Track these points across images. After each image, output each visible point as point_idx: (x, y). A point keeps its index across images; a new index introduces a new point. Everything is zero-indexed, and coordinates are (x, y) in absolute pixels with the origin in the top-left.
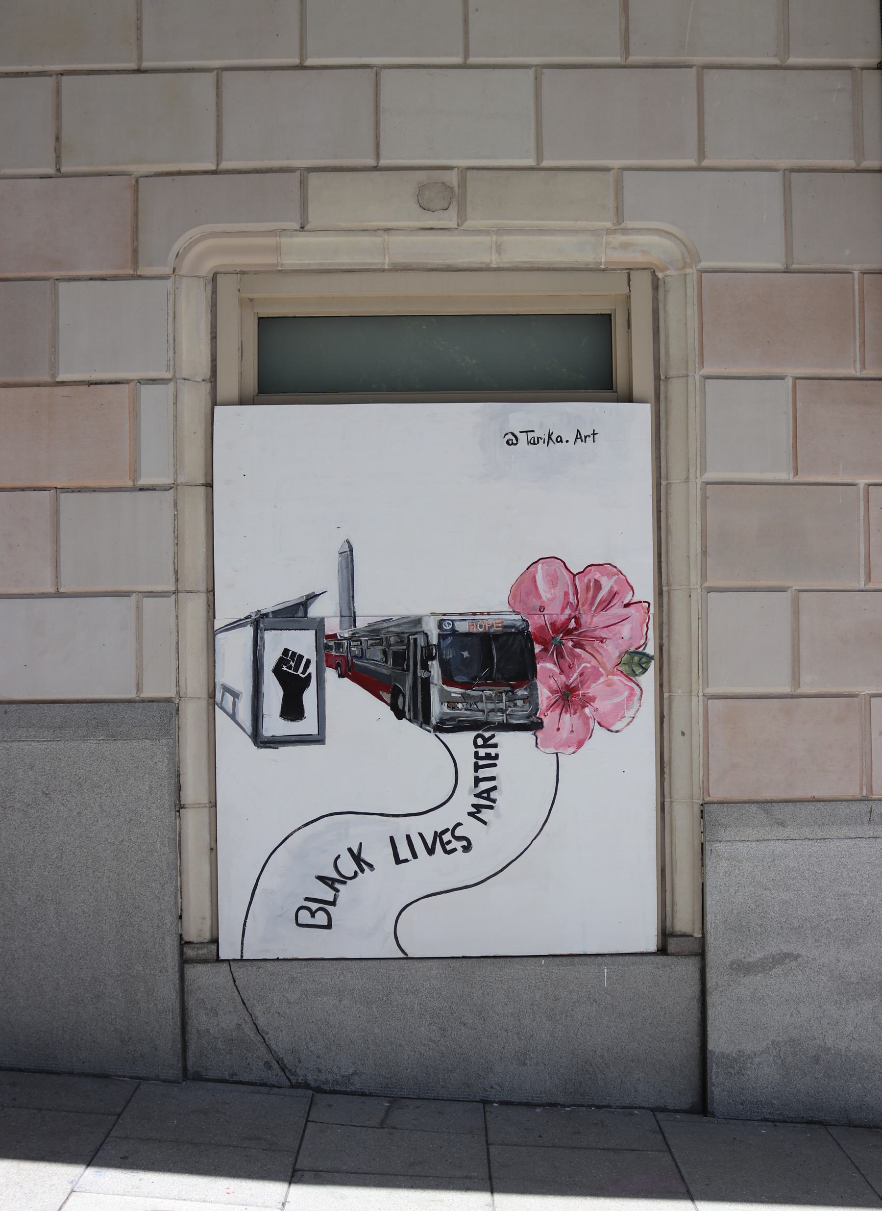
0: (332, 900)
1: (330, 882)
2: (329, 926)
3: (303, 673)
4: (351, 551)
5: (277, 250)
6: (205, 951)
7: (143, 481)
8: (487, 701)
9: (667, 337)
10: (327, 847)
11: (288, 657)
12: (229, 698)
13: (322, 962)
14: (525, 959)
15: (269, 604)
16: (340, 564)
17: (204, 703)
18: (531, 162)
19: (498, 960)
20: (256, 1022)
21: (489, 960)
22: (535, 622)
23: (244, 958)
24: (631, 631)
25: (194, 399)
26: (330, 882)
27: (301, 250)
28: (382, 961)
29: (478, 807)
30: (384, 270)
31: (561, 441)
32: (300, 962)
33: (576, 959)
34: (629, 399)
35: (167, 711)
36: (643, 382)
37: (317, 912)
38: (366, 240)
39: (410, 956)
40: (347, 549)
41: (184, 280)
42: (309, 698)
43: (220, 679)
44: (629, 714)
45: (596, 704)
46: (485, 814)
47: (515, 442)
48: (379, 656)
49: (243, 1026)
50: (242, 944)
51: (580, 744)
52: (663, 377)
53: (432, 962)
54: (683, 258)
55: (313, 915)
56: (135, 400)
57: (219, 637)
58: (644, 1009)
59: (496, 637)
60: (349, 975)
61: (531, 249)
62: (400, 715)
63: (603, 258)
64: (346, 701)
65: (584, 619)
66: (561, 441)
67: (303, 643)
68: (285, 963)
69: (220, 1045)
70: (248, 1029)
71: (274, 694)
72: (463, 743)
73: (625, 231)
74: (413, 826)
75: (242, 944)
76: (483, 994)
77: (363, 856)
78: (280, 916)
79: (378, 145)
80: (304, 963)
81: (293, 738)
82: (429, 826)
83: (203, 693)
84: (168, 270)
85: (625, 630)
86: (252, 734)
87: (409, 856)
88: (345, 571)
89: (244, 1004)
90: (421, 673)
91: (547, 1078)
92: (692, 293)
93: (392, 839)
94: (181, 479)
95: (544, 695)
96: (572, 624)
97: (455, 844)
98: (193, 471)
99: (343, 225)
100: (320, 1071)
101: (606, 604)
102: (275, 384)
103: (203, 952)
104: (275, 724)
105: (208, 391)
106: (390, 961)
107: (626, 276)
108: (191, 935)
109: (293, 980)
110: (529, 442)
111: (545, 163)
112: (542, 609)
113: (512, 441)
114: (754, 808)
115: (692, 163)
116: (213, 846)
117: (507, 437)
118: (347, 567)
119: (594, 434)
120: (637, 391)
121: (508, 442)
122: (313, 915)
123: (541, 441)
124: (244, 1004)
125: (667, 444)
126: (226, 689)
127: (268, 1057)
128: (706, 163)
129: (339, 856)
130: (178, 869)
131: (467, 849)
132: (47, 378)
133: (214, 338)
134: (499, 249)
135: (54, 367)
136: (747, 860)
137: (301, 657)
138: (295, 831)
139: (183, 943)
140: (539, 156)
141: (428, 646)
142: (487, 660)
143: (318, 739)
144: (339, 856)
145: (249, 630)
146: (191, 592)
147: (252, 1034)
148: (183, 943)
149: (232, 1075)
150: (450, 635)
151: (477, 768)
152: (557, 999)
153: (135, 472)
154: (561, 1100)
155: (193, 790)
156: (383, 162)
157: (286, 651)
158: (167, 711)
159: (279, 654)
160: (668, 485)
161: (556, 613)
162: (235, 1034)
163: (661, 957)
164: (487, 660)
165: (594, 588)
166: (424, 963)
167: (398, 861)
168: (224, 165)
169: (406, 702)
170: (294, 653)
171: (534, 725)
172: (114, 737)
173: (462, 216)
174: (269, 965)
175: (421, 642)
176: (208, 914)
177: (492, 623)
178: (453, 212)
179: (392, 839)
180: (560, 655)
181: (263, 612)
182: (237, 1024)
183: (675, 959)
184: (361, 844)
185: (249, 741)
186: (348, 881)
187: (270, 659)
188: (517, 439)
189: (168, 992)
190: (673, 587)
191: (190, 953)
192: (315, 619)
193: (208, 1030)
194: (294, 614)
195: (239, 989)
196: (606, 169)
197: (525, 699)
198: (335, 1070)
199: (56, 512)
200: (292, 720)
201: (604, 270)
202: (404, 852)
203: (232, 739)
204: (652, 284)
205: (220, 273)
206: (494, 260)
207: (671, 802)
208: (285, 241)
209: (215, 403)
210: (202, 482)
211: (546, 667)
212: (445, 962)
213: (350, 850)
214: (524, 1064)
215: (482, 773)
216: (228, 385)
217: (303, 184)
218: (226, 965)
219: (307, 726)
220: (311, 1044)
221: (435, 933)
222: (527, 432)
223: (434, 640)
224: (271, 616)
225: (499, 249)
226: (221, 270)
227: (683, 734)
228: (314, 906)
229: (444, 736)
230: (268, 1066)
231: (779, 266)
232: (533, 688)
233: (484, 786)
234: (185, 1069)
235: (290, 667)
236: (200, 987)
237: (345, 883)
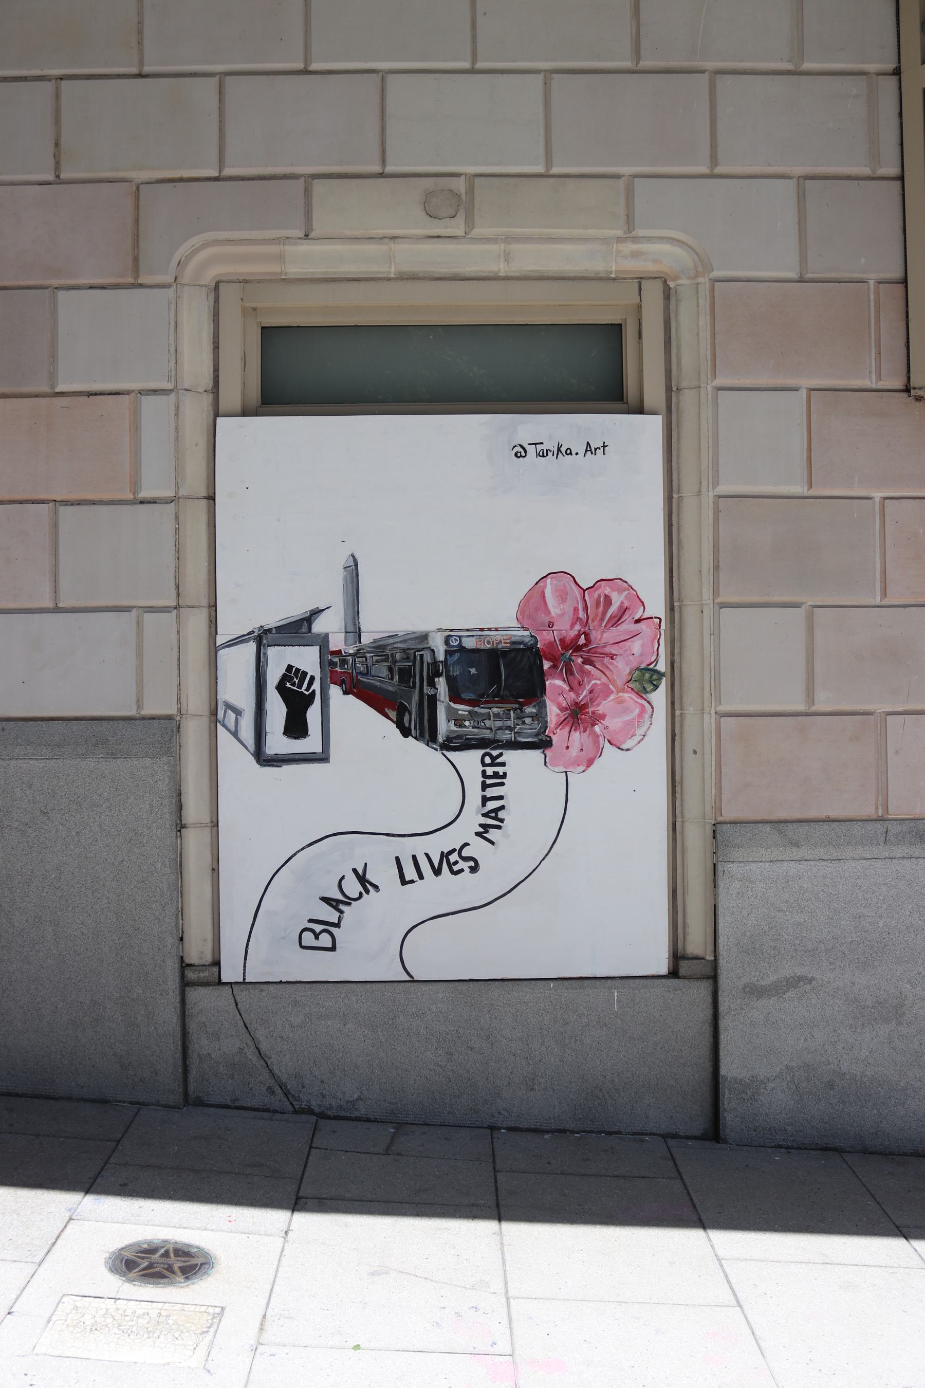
0: (336, 921)
1: (334, 904)
2: (333, 948)
3: (307, 690)
4: (356, 565)
5: (281, 258)
6: (207, 974)
7: (144, 494)
8: (495, 719)
9: (679, 348)
10: (331, 868)
11: (292, 674)
12: (232, 716)
13: (326, 985)
14: (533, 982)
15: (272, 620)
16: (345, 579)
17: (205, 721)
18: (540, 169)
19: (506, 983)
22: (544, 638)
24: (641, 648)
25: (195, 410)
26: (334, 904)
27: (306, 258)
29: (486, 827)
30: (390, 279)
31: (571, 454)
32: (304, 985)
33: (586, 982)
34: (640, 410)
35: (167, 729)
36: (654, 393)
37: (321, 934)
38: (371, 248)
39: (416, 979)
40: (351, 563)
41: (186, 288)
42: (313, 715)
43: (223, 696)
44: (641, 731)
45: (606, 722)
46: (493, 834)
47: (523, 454)
48: (385, 673)
50: (245, 966)
51: (590, 763)
52: (674, 389)
53: (438, 985)
55: (317, 936)
56: (136, 412)
57: (221, 653)
59: (504, 653)
61: (540, 258)
62: (406, 733)
63: (614, 267)
65: (594, 635)
66: (571, 454)
67: (307, 659)
70: (251, 1053)
72: (470, 762)
73: (635, 240)
74: (420, 846)
75: (245, 966)
76: (491, 1018)
78: (283, 938)
79: (383, 152)
80: (308, 985)
81: (297, 757)
82: (436, 846)
83: (205, 710)
84: (169, 279)
85: (636, 646)
87: (416, 877)
88: (350, 586)
90: (427, 690)
91: (556, 1103)
92: (704, 303)
93: (397, 859)
94: (183, 492)
95: (553, 712)
96: (582, 640)
97: (462, 865)
98: (195, 483)
99: (348, 233)
100: (324, 1096)
101: (617, 620)
102: (279, 394)
103: (205, 975)
106: (396, 984)
107: (637, 285)
108: (193, 958)
109: (296, 1003)
110: (538, 455)
111: (555, 170)
112: (551, 625)
114: (767, 828)
115: (704, 169)
117: (516, 449)
118: (352, 582)
119: (604, 446)
120: (648, 403)
121: (516, 455)
122: (317, 936)
123: (550, 454)
125: (678, 457)
126: (228, 706)
127: (271, 1082)
128: (718, 170)
130: (179, 890)
131: (474, 869)
132: (46, 389)
133: (216, 347)
134: (507, 257)
135: (53, 377)
136: (759, 882)
137: (305, 674)
138: (298, 852)
139: (184, 966)
140: (549, 162)
141: (435, 663)
142: (495, 677)
143: (322, 758)
145: (252, 646)
148: (184, 966)
149: (234, 1101)
150: (456, 651)
151: (484, 786)
153: (136, 485)
154: (571, 1126)
155: (195, 810)
156: (389, 169)
157: (290, 668)
158: (167, 729)
159: (283, 670)
160: (680, 499)
161: (565, 628)
162: (237, 1059)
164: (495, 677)
165: (605, 604)
167: (404, 882)
168: (227, 172)
169: (410, 719)
170: (298, 670)
171: (542, 744)
172: (114, 756)
173: (470, 224)
174: (272, 988)
175: (428, 658)
176: (209, 936)
177: (500, 639)
178: (460, 219)
179: (397, 859)
180: (569, 671)
181: (266, 628)
182: (239, 1048)
183: (686, 982)
185: (252, 759)
189: (168, 1014)
190: (685, 603)
191: (191, 975)
192: (319, 635)
193: (209, 1054)
194: (298, 630)
196: (617, 177)
197: (533, 717)
198: (340, 1095)
199: (55, 526)
200: (296, 738)
201: (614, 279)
202: (410, 873)
203: (235, 757)
205: (223, 282)
206: (502, 269)
207: (683, 822)
208: (289, 249)
209: (217, 414)
210: (204, 495)
211: (555, 683)
212: (452, 985)
213: (355, 871)
214: (533, 1089)
215: (490, 792)
216: (231, 396)
217: (308, 192)
218: (228, 988)
219: (311, 744)
221: (444, 955)
222: (536, 444)
223: (441, 657)
224: (274, 631)
225: (507, 257)
227: (695, 752)
228: (318, 928)
229: (451, 755)
230: (271, 1091)
231: (793, 275)
232: (542, 706)
233: (491, 805)
234: (186, 1094)
235: (293, 684)
236: (201, 1011)
237: (349, 904)
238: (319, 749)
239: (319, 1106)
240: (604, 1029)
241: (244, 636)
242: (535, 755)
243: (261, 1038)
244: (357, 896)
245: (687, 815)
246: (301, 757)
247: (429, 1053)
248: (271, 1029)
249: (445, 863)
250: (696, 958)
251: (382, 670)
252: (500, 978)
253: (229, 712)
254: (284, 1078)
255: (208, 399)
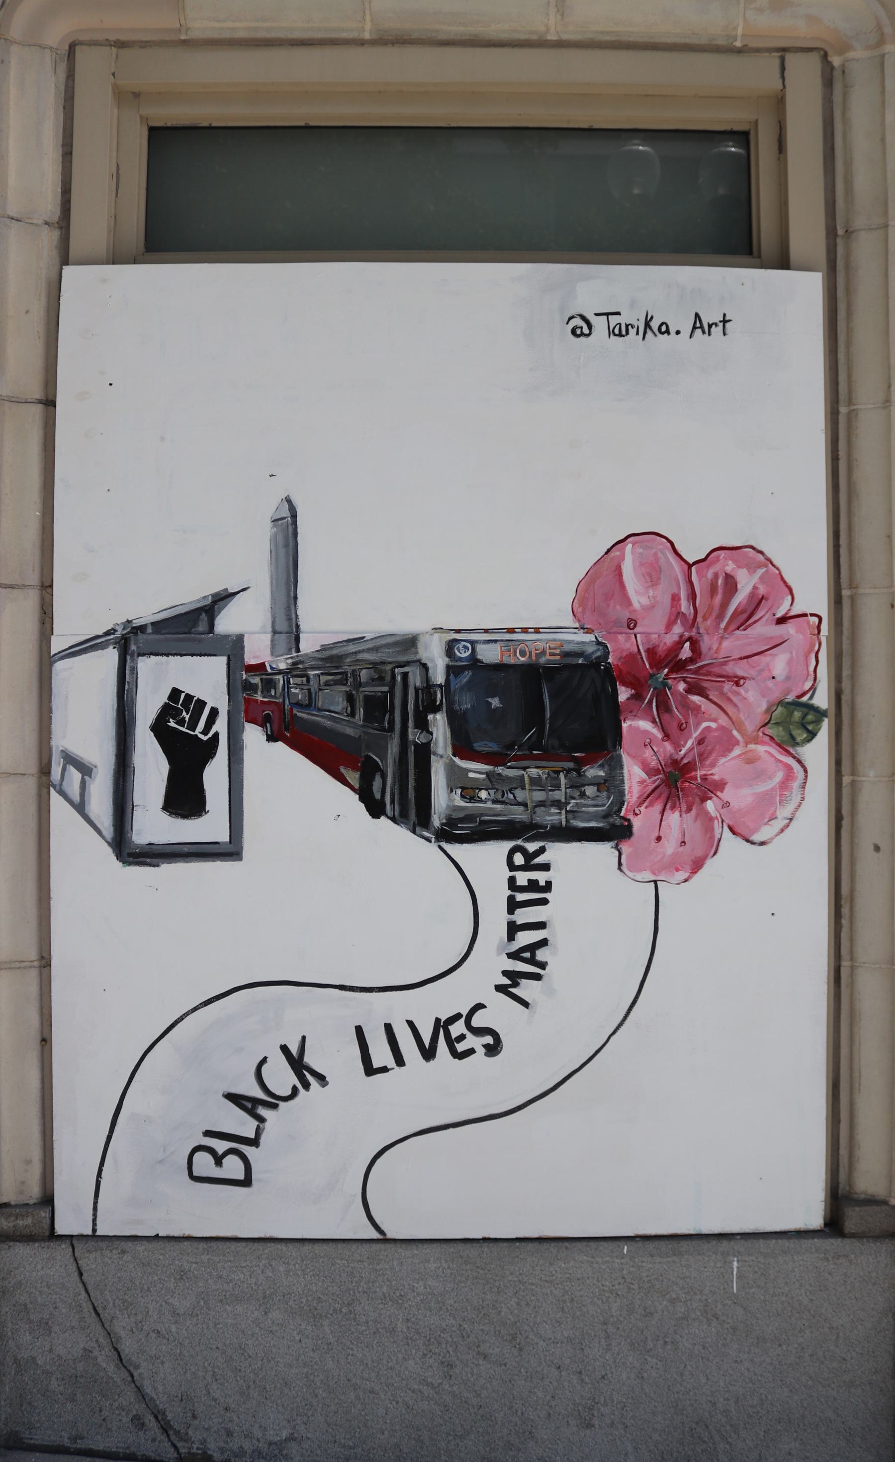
0: (253, 1136)
1: (249, 1105)
2: (247, 1182)
3: (205, 732)
4: (294, 516)
6: (29, 1221)
8: (532, 785)
9: (848, 163)
11: (179, 704)
13: (233, 1246)
14: (593, 1244)
16: (274, 540)
17: (31, 784)
19: (546, 1245)
20: (118, 1347)
21: (530, 1246)
22: (620, 647)
23: (98, 1233)
26: (249, 1105)
28: (340, 1246)
29: (514, 977)
30: (362, 43)
31: (668, 332)
32: (195, 1244)
33: (685, 1245)
39: (389, 1235)
40: (285, 512)
41: (15, 49)
44: (784, 812)
45: (727, 794)
46: (526, 989)
47: (586, 330)
48: (340, 704)
49: (96, 1353)
50: (95, 1209)
51: (697, 866)
52: (840, 232)
53: (427, 1249)
54: (879, 27)
55: (218, 1160)
57: (60, 667)
58: (801, 1331)
60: (282, 1269)
62: (375, 809)
64: (281, 784)
65: (707, 643)
66: (668, 332)
67: (205, 679)
68: (169, 1246)
69: (54, 1385)
71: (152, 767)
72: (488, 861)
74: (398, 1009)
75: (95, 1209)
76: (518, 1304)
77: (308, 1059)
78: (161, 1162)
80: (202, 1245)
81: (186, 849)
82: (427, 1008)
85: (779, 663)
86: (114, 839)
87: (390, 1062)
88: (282, 551)
89: (98, 1314)
90: (415, 736)
91: (630, 1449)
93: (359, 1030)
95: (634, 776)
96: (686, 652)
97: (472, 1041)
100: (229, 1433)
101: (746, 618)
104: (153, 824)
105: (55, 243)
106: (354, 1246)
107: (777, 62)
109: (182, 1275)
110: (611, 333)
112: (632, 624)
113: (581, 329)
116: (46, 1036)
117: (573, 323)
118: (286, 546)
119: (725, 321)
120: (796, 250)
121: (573, 332)
122: (218, 1160)
123: (632, 332)
124: (98, 1314)
125: (848, 344)
127: (139, 1408)
129: (264, 1060)
131: (493, 1050)
133: (67, 154)
137: (201, 704)
138: (187, 1014)
141: (428, 687)
142: (533, 713)
143: (230, 851)
144: (264, 1060)
145: (111, 655)
146: (11, 587)
147: (109, 1366)
149: (74, 1439)
150: (467, 667)
151: (513, 905)
152: (648, 1314)
157: (175, 693)
159: (164, 699)
160: (852, 416)
161: (656, 631)
162: (80, 1367)
163: (832, 1241)
164: (533, 713)
165: (725, 590)
166: (415, 1250)
167: (370, 1070)
169: (385, 787)
170: (189, 697)
171: (615, 831)
174: (141, 1247)
175: (416, 679)
176: (36, 1155)
179: (359, 1030)
180: (664, 706)
181: (136, 623)
182: (85, 1350)
183: (856, 1243)
184: (304, 1038)
185: (108, 852)
186: (282, 1104)
187: (147, 708)
188: (590, 326)
190: (861, 591)
192: (226, 637)
193: (34, 1359)
194: (190, 628)
195: (90, 1288)
197: (600, 785)
198: (258, 1433)
200: (185, 817)
201: (740, 51)
202: (381, 1055)
204: (823, 76)
205: (81, 43)
207: (852, 968)
210: (39, 397)
211: (638, 726)
212: (451, 1249)
213: (284, 1049)
214: (589, 1426)
215: (523, 916)
218: (65, 1247)
219: (211, 827)
220: (214, 1386)
222: (607, 314)
223: (439, 678)
224: (149, 630)
226: (82, 38)
227: (877, 848)
228: (221, 1146)
229: (454, 849)
230: (138, 1422)
232: (616, 765)
233: (525, 938)
235: (181, 722)
236: (20, 1283)
237: (274, 1106)
238: (222, 835)
239: (222, 1450)
240: (714, 1323)
241: (98, 637)
242: (604, 851)
243: (122, 1334)
244: (288, 1092)
245: (862, 956)
246: (193, 849)
247: (411, 1362)
248: (139, 1317)
249: (443, 1038)
250: (871, 1201)
251: (335, 700)
252: (536, 1235)
253: (71, 769)
254: (162, 1402)
255: (49, 238)
